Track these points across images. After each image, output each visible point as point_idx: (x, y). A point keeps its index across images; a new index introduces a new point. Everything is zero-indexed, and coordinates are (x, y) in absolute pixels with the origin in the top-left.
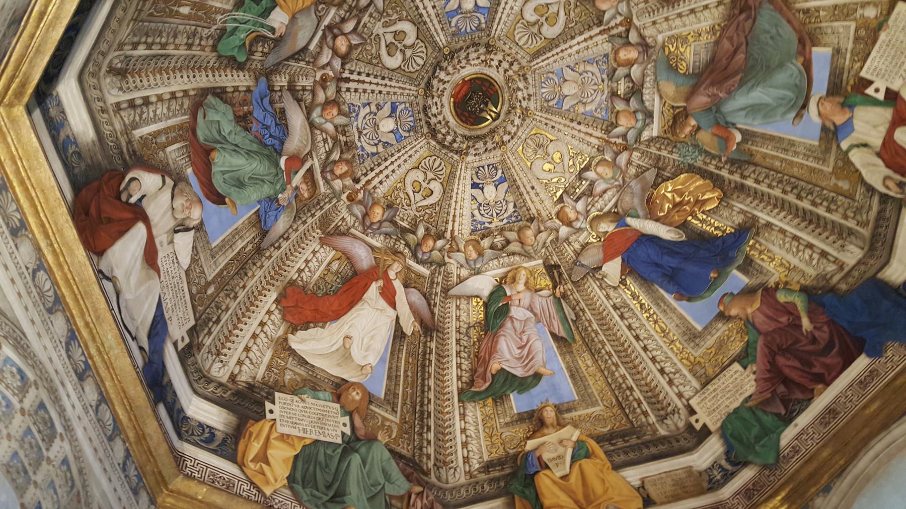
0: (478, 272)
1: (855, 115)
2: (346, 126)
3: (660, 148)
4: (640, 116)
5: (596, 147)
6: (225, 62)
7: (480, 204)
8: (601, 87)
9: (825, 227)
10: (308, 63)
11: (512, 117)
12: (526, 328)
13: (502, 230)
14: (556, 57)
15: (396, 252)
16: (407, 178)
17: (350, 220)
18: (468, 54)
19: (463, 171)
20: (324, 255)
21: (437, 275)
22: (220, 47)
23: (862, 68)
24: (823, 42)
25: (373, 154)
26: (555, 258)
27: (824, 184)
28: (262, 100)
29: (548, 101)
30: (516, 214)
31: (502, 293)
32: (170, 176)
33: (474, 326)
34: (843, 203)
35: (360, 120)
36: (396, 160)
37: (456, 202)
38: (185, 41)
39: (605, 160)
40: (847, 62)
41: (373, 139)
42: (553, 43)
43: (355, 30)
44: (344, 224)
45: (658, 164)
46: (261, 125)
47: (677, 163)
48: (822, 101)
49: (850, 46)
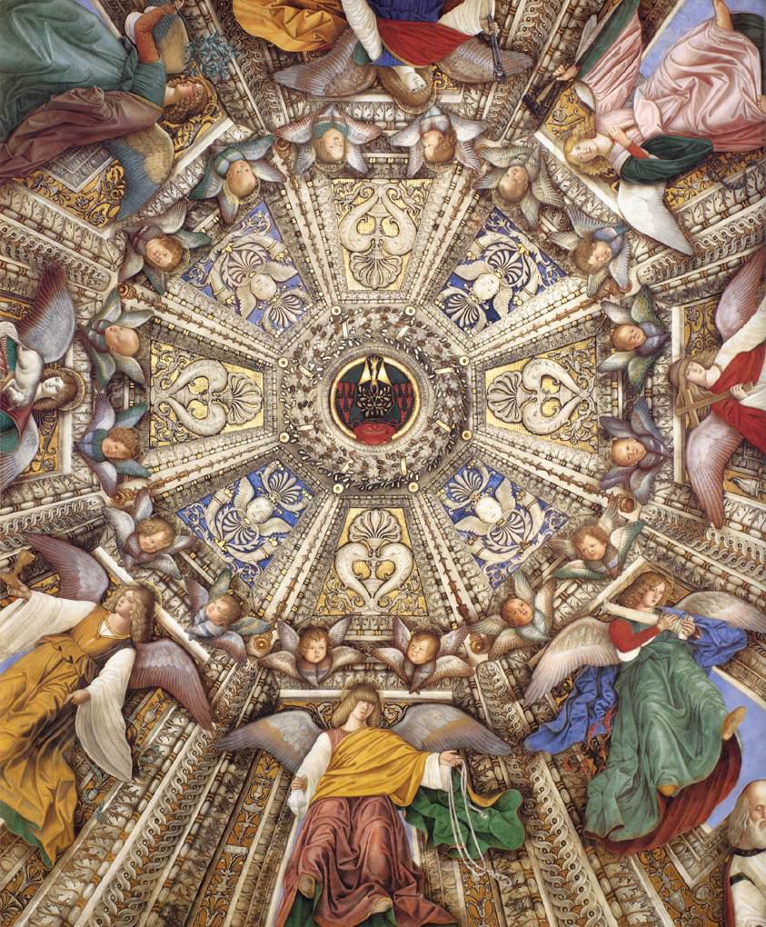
0: (624, 226)
2: (525, 574)
3: (241, 97)
4: (223, 165)
5: (310, 184)
6: (532, 822)
7: (515, 289)
8: (229, 249)
10: (472, 686)
11: (360, 332)
12: (666, 91)
13: (532, 230)
14: (239, 338)
15: (673, 386)
16: (546, 431)
17: (662, 491)
18: (322, 457)
19: (484, 348)
20: (741, 512)
21: (671, 292)
22: (515, 846)
25: (543, 506)
26: (518, 115)
28: (557, 734)
29: (304, 303)
30: (492, 224)
31: (633, 166)
32: (726, 866)
33: (721, 180)
35: (506, 557)
36: (531, 464)
37: (535, 329)
38: (529, 913)
39: (318, 157)
41: (522, 520)
42: (225, 357)
43: (392, 643)
44: (674, 497)
45: (266, 79)
46: (592, 721)
47: (242, 57)
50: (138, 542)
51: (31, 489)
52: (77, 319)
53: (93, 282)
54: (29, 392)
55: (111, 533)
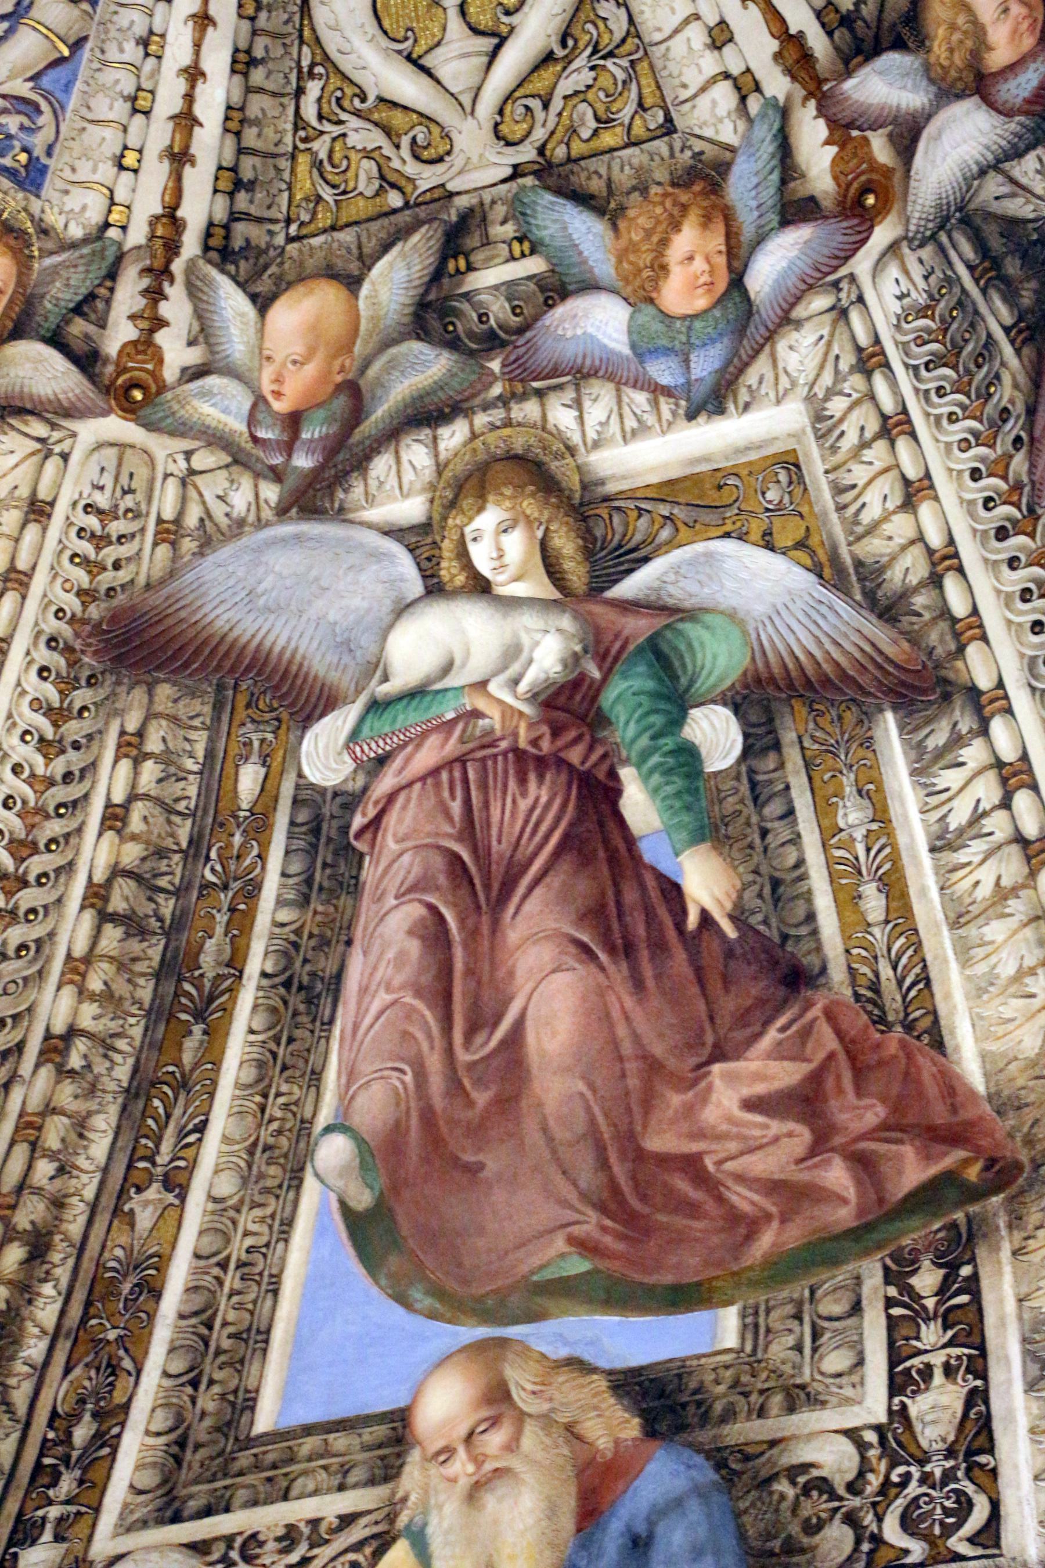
50: (1012, 68)
51: (873, 529)
52: (261, 524)
53: (129, 501)
54: (528, 621)
55: (993, 186)
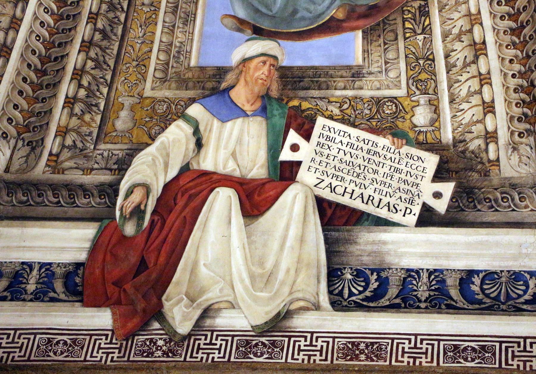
1: (251, 119)
9: (36, 100)
23: (331, 118)
24: (373, 48)
27: (119, 85)
34: (89, 125)
40: (338, 93)
48: (272, 61)
49: (367, 93)
